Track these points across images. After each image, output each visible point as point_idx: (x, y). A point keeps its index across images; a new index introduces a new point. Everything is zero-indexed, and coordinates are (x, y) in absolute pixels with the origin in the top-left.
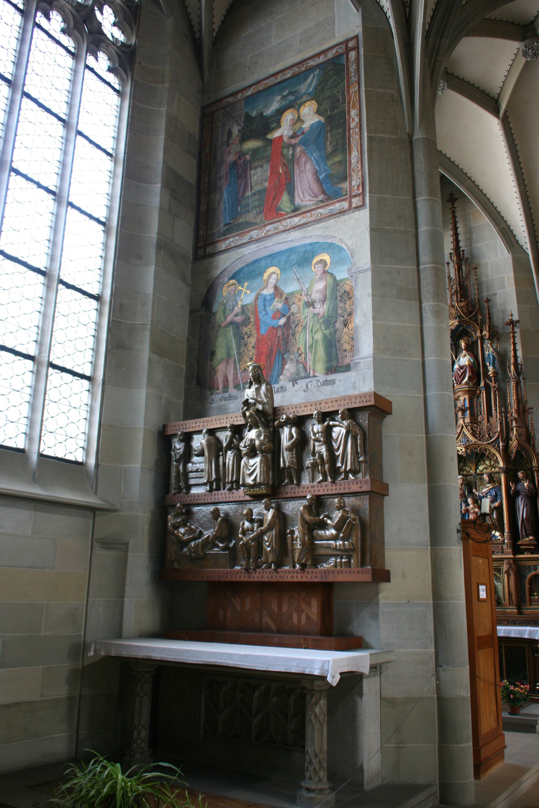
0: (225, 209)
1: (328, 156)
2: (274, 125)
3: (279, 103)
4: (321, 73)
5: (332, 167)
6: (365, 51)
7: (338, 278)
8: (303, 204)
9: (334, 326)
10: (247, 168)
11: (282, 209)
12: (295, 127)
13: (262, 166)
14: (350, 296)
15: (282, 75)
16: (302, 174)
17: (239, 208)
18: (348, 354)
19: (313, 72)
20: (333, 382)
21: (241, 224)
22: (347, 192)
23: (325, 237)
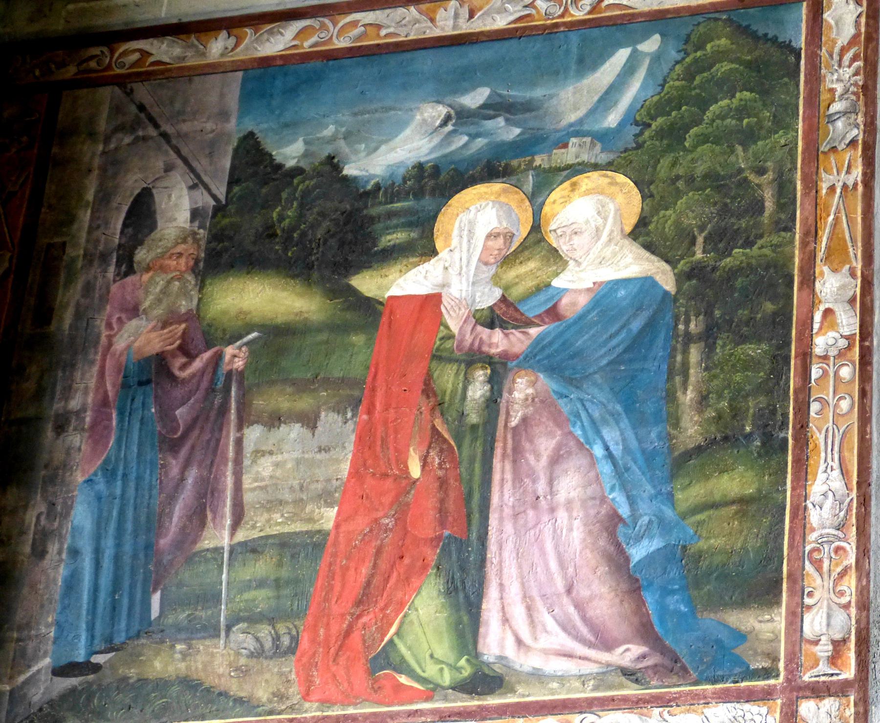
0: (71, 585)
2: (398, 237)
3: (436, 140)
4: (674, 55)
5: (700, 517)
8: (526, 662)
10: (223, 410)
11: (403, 660)
12: (511, 274)
13: (310, 421)
15: (465, 12)
16: (531, 513)
17: (156, 599)
19: (633, 41)
21: (162, 685)
22: (776, 660)
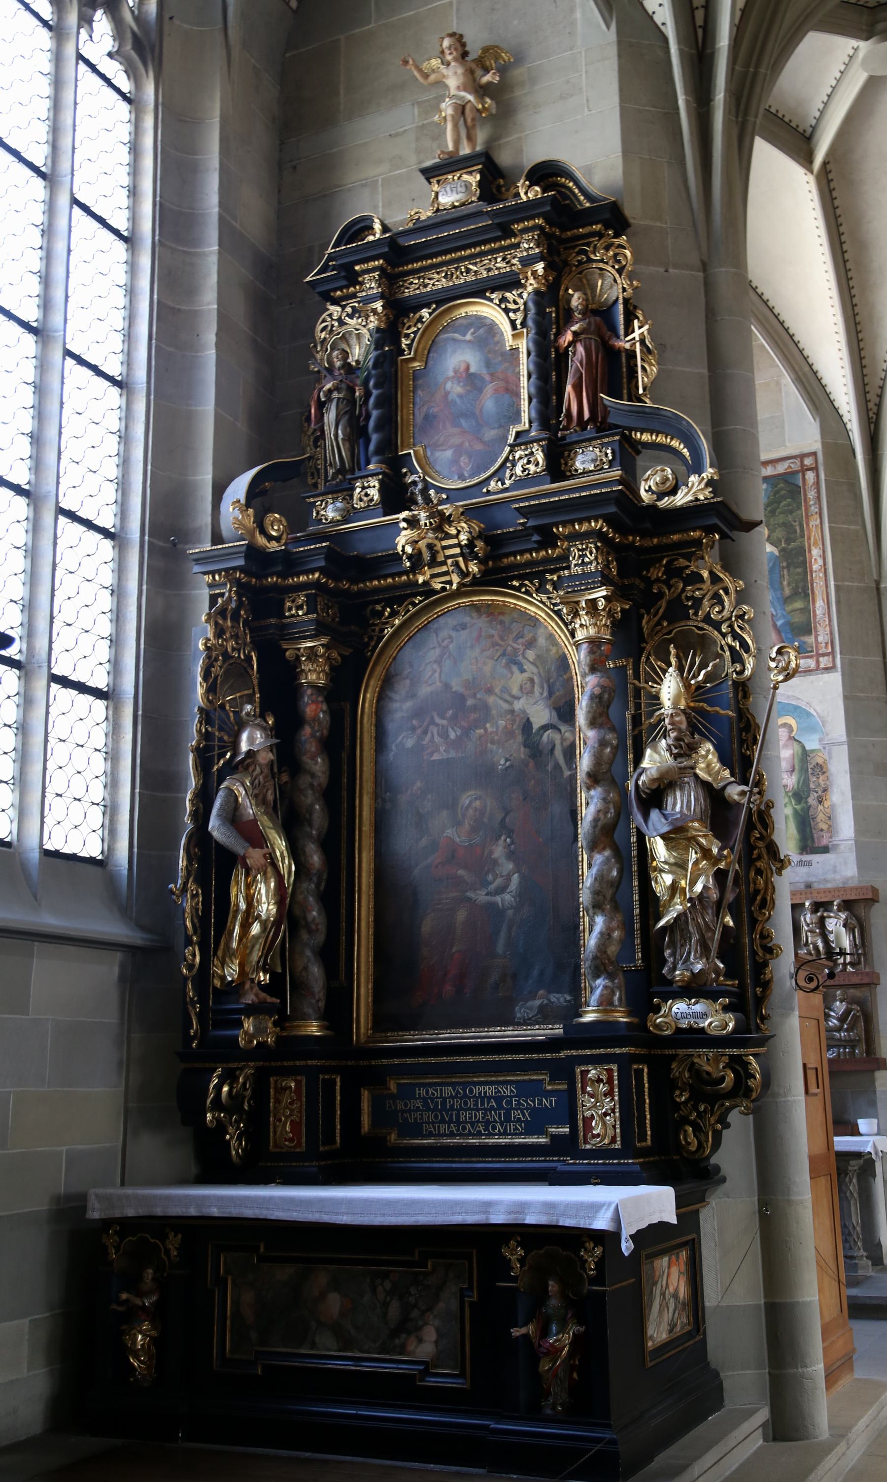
1: (786, 600)
6: (826, 476)
7: (807, 748)
9: (807, 802)
20: (809, 864)
23: (788, 697)
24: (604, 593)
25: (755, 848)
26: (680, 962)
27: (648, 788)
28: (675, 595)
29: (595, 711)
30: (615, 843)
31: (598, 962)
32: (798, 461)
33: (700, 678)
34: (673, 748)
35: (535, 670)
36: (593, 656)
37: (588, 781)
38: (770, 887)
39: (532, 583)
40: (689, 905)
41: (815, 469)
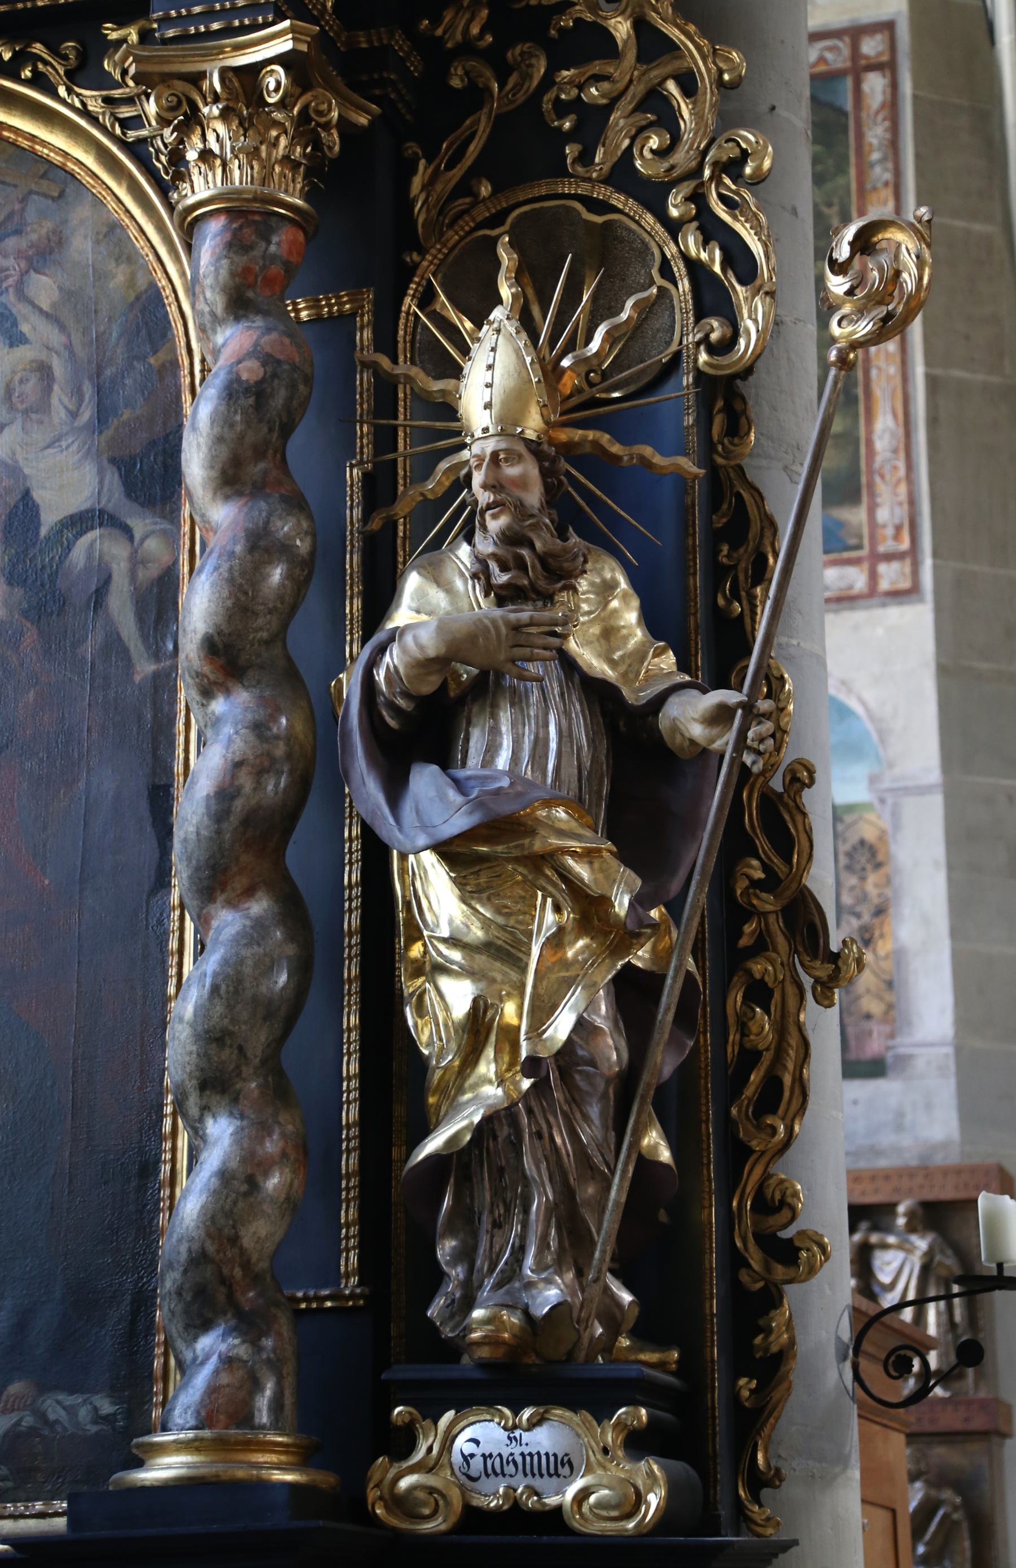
6: (916, 86)
14: (880, 857)
18: (877, 1029)
24: (284, 45)
25: (747, 914)
26: (489, 1283)
27: (406, 694)
28: (521, 98)
29: (241, 438)
30: (287, 878)
31: (209, 1271)
32: (844, 46)
33: (595, 346)
34: (493, 566)
35: (55, 337)
36: (242, 260)
37: (206, 669)
38: (793, 1041)
39: (54, 51)
40: (526, 1084)
41: (888, 66)
